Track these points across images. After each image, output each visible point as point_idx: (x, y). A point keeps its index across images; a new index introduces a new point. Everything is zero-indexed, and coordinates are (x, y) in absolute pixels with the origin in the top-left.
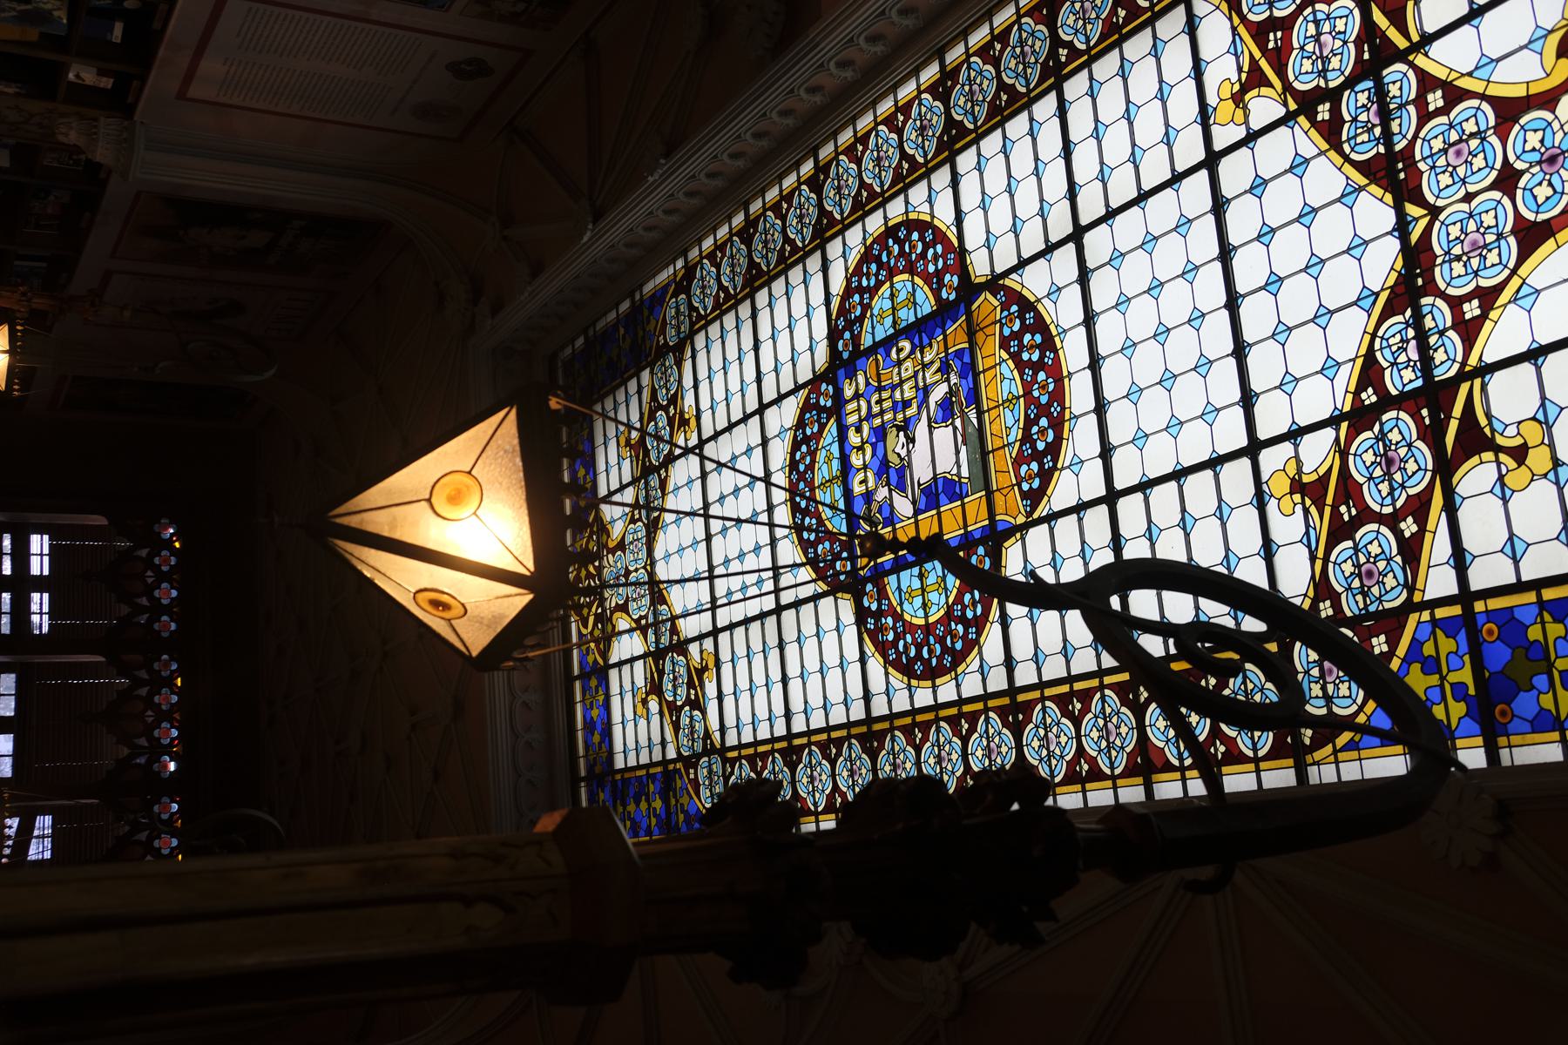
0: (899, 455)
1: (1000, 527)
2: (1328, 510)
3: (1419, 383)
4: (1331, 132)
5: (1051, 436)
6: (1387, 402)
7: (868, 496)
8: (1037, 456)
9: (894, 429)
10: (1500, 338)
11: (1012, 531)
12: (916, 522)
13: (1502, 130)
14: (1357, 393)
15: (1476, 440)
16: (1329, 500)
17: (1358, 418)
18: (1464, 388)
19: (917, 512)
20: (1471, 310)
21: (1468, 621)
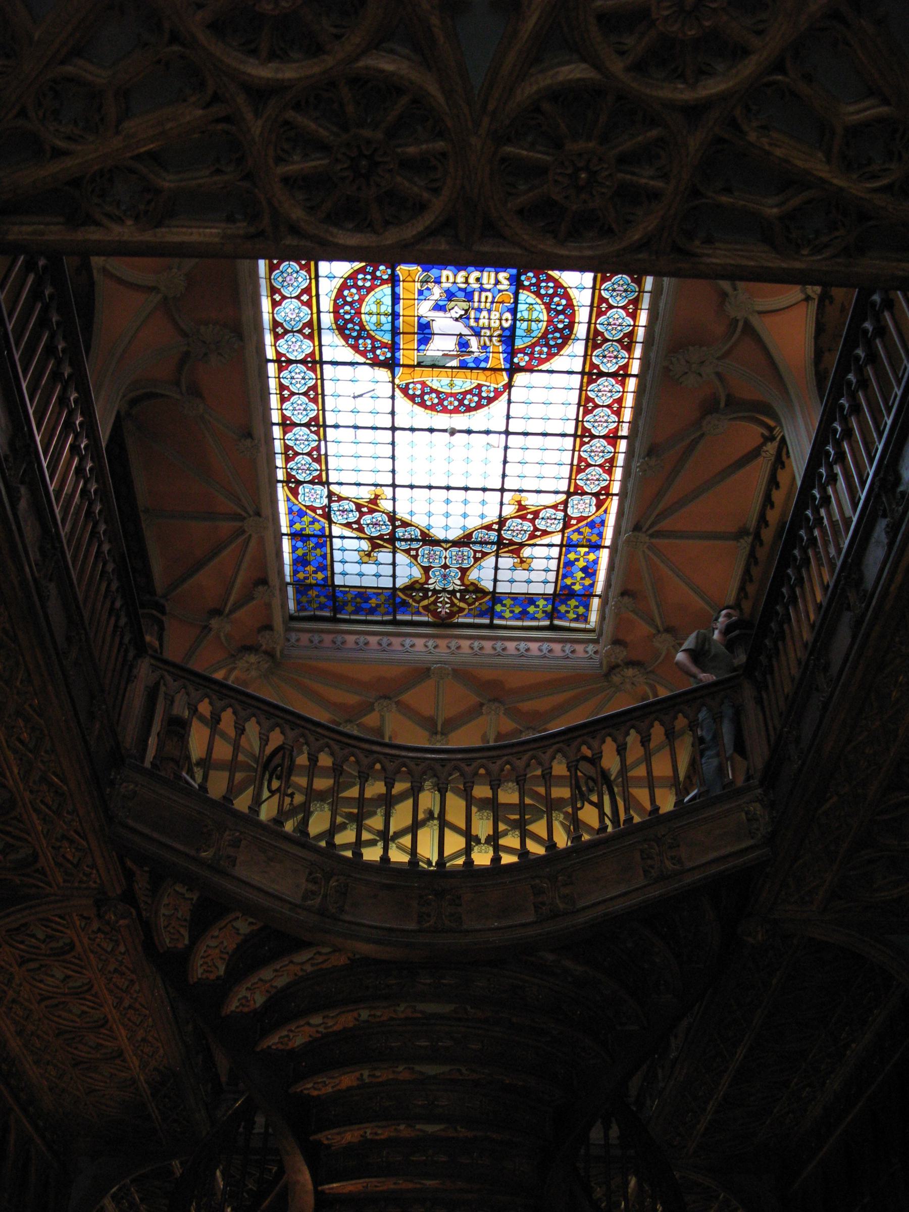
0: (453, 308)
1: (397, 369)
2: (366, 504)
3: (397, 536)
4: (488, 528)
5: (429, 403)
6: (395, 527)
7: (438, 281)
8: (422, 396)
9: (467, 308)
10: (401, 558)
11: (393, 377)
12: (414, 316)
13: (461, 569)
14: (400, 520)
15: (375, 546)
16: (370, 505)
17: (392, 517)
18: (391, 547)
19: (420, 317)
20: (413, 553)
21: (324, 536)
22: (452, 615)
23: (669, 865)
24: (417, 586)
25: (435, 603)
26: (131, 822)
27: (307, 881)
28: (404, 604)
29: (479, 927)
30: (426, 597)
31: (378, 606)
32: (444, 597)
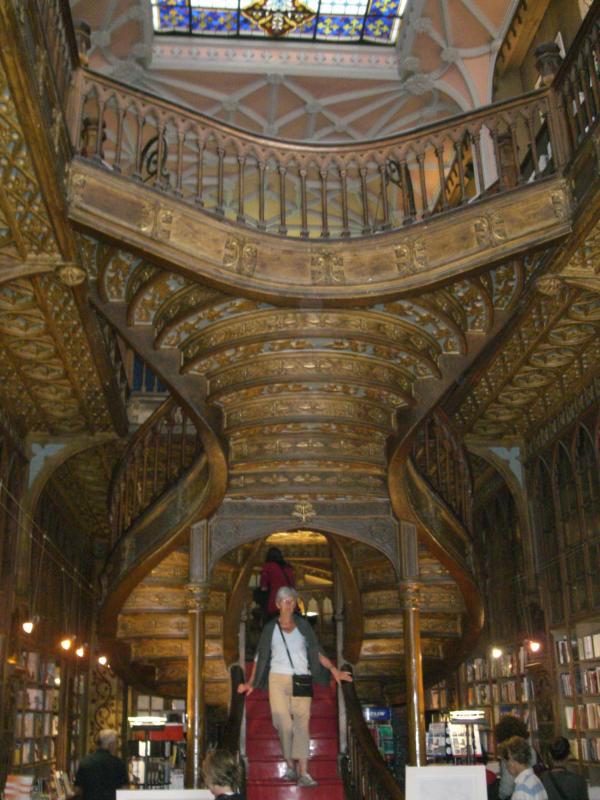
22: (284, 31)
23: (497, 237)
24: (257, 7)
25: (271, 21)
26: (84, 206)
27: (226, 247)
28: (246, 21)
29: (358, 281)
30: (264, 16)
31: (225, 23)
32: (278, 17)
